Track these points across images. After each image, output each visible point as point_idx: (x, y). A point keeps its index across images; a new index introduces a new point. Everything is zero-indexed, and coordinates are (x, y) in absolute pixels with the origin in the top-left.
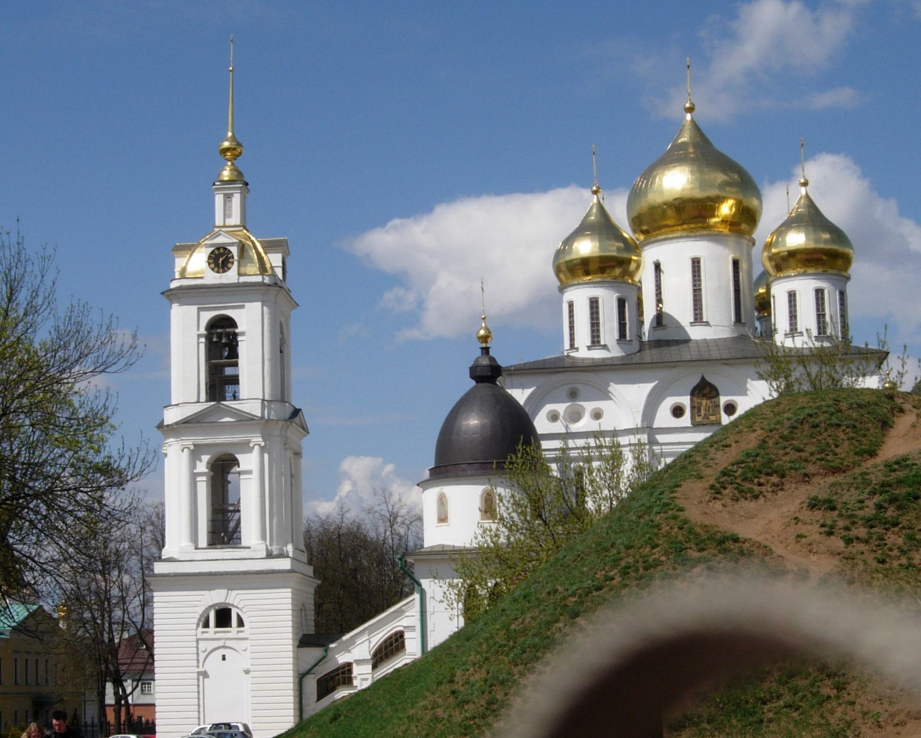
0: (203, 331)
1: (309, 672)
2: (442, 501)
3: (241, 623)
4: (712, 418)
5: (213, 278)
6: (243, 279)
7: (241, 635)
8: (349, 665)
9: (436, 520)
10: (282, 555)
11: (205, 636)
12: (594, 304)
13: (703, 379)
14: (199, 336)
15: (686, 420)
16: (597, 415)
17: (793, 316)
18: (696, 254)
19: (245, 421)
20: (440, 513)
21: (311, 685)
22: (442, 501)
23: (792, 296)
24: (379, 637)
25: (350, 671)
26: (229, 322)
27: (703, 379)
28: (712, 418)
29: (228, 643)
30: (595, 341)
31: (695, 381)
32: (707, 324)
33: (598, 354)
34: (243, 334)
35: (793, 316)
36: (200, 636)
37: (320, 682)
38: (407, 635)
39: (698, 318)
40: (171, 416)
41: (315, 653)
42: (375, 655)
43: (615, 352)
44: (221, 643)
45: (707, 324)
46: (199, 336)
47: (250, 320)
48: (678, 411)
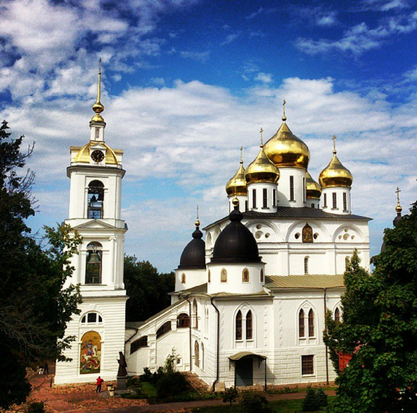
1: (128, 341)
2: (224, 272)
3: (100, 320)
5: (92, 163)
6: (107, 165)
7: (100, 326)
9: (220, 280)
10: (120, 289)
12: (265, 191)
13: (307, 224)
14: (86, 188)
19: (109, 228)
21: (129, 346)
22: (224, 272)
25: (146, 340)
29: (94, 330)
30: (265, 206)
31: (304, 225)
32: (295, 202)
33: (265, 211)
34: (107, 189)
36: (80, 326)
37: (132, 345)
38: (172, 323)
39: (292, 199)
41: (132, 332)
43: (272, 210)
44: (90, 330)
45: (295, 202)
46: (86, 188)
48: (297, 236)
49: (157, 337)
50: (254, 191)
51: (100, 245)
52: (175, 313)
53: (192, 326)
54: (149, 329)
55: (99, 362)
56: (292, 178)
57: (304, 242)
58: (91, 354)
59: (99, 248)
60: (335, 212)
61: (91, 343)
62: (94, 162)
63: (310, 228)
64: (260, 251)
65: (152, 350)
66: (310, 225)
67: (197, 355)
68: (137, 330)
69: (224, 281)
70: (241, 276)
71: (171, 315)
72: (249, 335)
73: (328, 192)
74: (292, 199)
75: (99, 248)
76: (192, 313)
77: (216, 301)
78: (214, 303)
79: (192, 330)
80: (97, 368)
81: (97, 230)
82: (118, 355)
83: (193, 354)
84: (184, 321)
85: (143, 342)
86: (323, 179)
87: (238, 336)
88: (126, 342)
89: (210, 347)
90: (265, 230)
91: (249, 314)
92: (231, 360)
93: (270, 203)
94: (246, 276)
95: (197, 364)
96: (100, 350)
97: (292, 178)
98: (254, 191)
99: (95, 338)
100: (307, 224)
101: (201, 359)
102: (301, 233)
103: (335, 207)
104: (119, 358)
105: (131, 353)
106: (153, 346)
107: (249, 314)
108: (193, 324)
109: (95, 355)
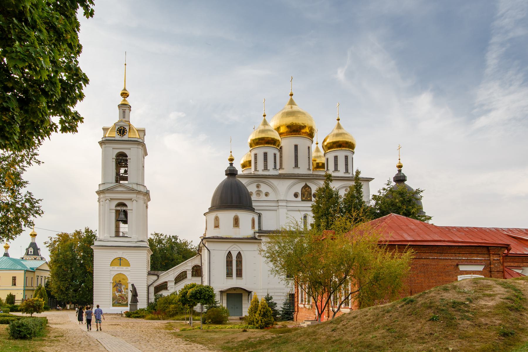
2: (217, 219)
4: (309, 199)
11: (113, 269)
12: (265, 155)
13: (306, 184)
15: (299, 198)
16: (267, 195)
18: (296, 143)
22: (217, 219)
27: (306, 184)
28: (309, 199)
30: (266, 168)
31: (303, 184)
36: (111, 269)
44: (119, 272)
48: (296, 195)
51: (125, 205)
55: (127, 298)
56: (296, 147)
57: (302, 200)
58: (120, 291)
59: (125, 208)
62: (119, 136)
63: (309, 187)
66: (309, 184)
70: (232, 222)
72: (239, 274)
74: (296, 166)
75: (125, 208)
80: (125, 303)
81: (122, 192)
87: (229, 274)
88: (149, 287)
90: (264, 188)
91: (239, 255)
92: (221, 292)
97: (296, 147)
99: (123, 279)
100: (306, 186)
103: (336, 169)
107: (239, 255)
109: (123, 293)
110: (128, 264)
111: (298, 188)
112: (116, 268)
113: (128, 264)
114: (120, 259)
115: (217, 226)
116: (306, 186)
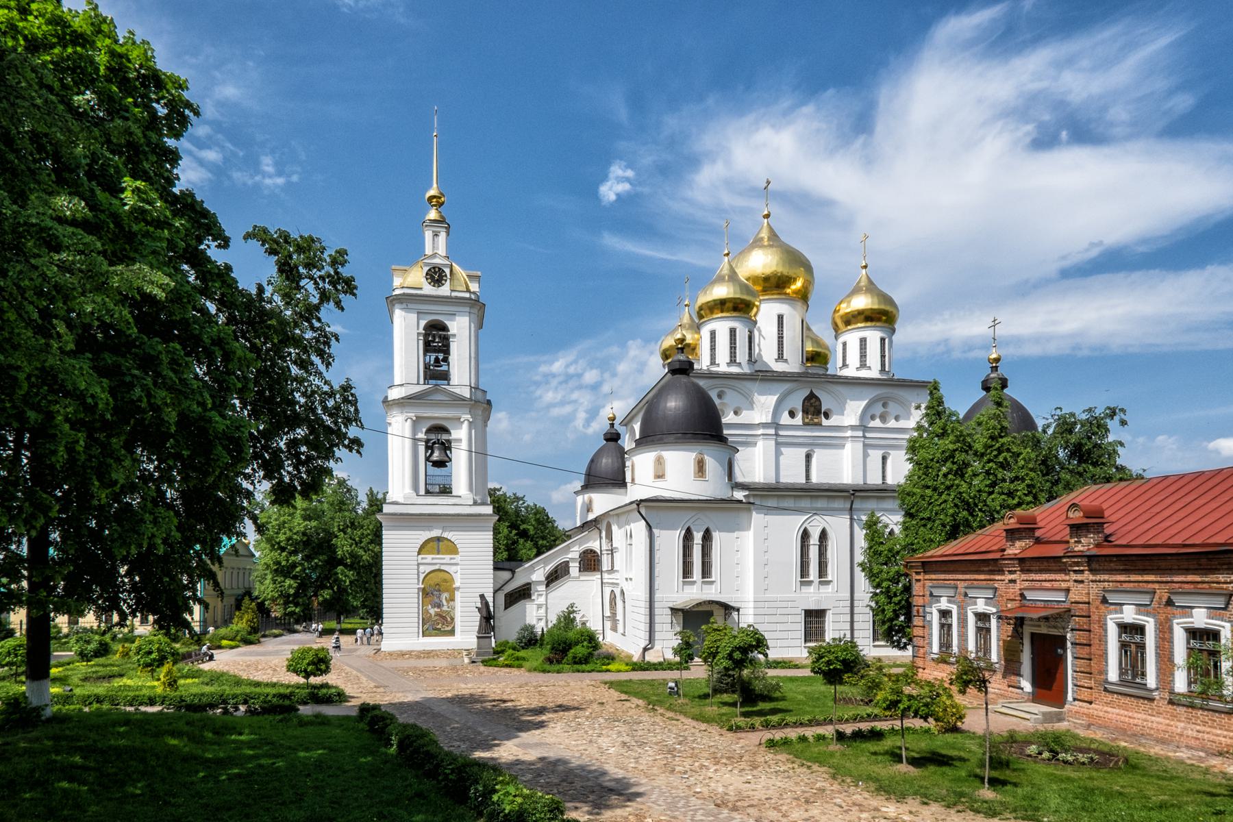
0: (421, 330)
2: (659, 462)
8: (529, 584)
12: (733, 332)
15: (799, 419)
17: (863, 355)
18: (781, 312)
20: (656, 470)
22: (659, 462)
23: (863, 342)
24: (550, 567)
25: (529, 589)
26: (444, 328)
29: (443, 567)
30: (733, 360)
31: (806, 393)
32: (786, 361)
33: (734, 370)
35: (863, 355)
39: (780, 357)
40: (394, 394)
41: (506, 575)
42: (547, 578)
44: (437, 567)
45: (786, 361)
47: (460, 327)
48: (792, 414)
49: (547, 586)
50: (713, 334)
52: (576, 548)
53: (604, 569)
54: (536, 571)
55: (453, 619)
56: (780, 318)
58: (439, 606)
60: (864, 374)
61: (435, 590)
63: (818, 399)
64: (725, 432)
65: (539, 606)
66: (817, 393)
67: (614, 614)
68: (513, 572)
69: (660, 476)
71: (572, 553)
72: (706, 571)
73: (852, 338)
76: (604, 548)
77: (646, 507)
78: (643, 512)
79: (606, 576)
82: (478, 599)
83: (608, 613)
84: (590, 562)
85: (524, 593)
86: (842, 317)
87: (687, 571)
88: (495, 592)
89: (637, 591)
93: (742, 356)
94: (701, 467)
95: (614, 629)
96: (453, 600)
98: (713, 334)
99: (445, 581)
100: (812, 396)
101: (619, 617)
102: (800, 408)
104: (479, 605)
105: (506, 608)
106: (542, 600)
108: (606, 566)
109: (445, 608)
110: (453, 550)
111: (797, 401)
112: (429, 558)
113: (453, 550)
114: (439, 539)
115: (660, 476)
116: (812, 396)
